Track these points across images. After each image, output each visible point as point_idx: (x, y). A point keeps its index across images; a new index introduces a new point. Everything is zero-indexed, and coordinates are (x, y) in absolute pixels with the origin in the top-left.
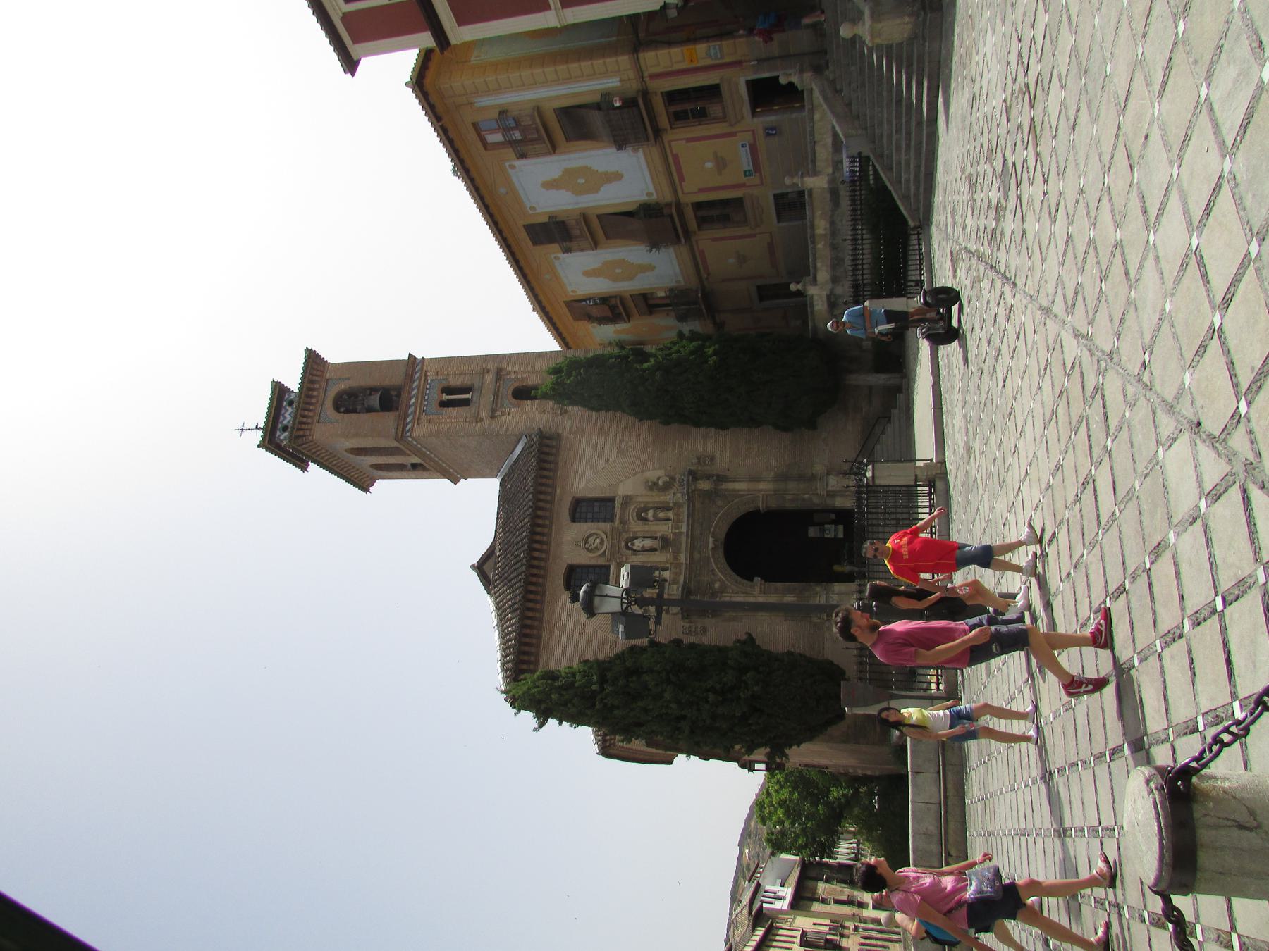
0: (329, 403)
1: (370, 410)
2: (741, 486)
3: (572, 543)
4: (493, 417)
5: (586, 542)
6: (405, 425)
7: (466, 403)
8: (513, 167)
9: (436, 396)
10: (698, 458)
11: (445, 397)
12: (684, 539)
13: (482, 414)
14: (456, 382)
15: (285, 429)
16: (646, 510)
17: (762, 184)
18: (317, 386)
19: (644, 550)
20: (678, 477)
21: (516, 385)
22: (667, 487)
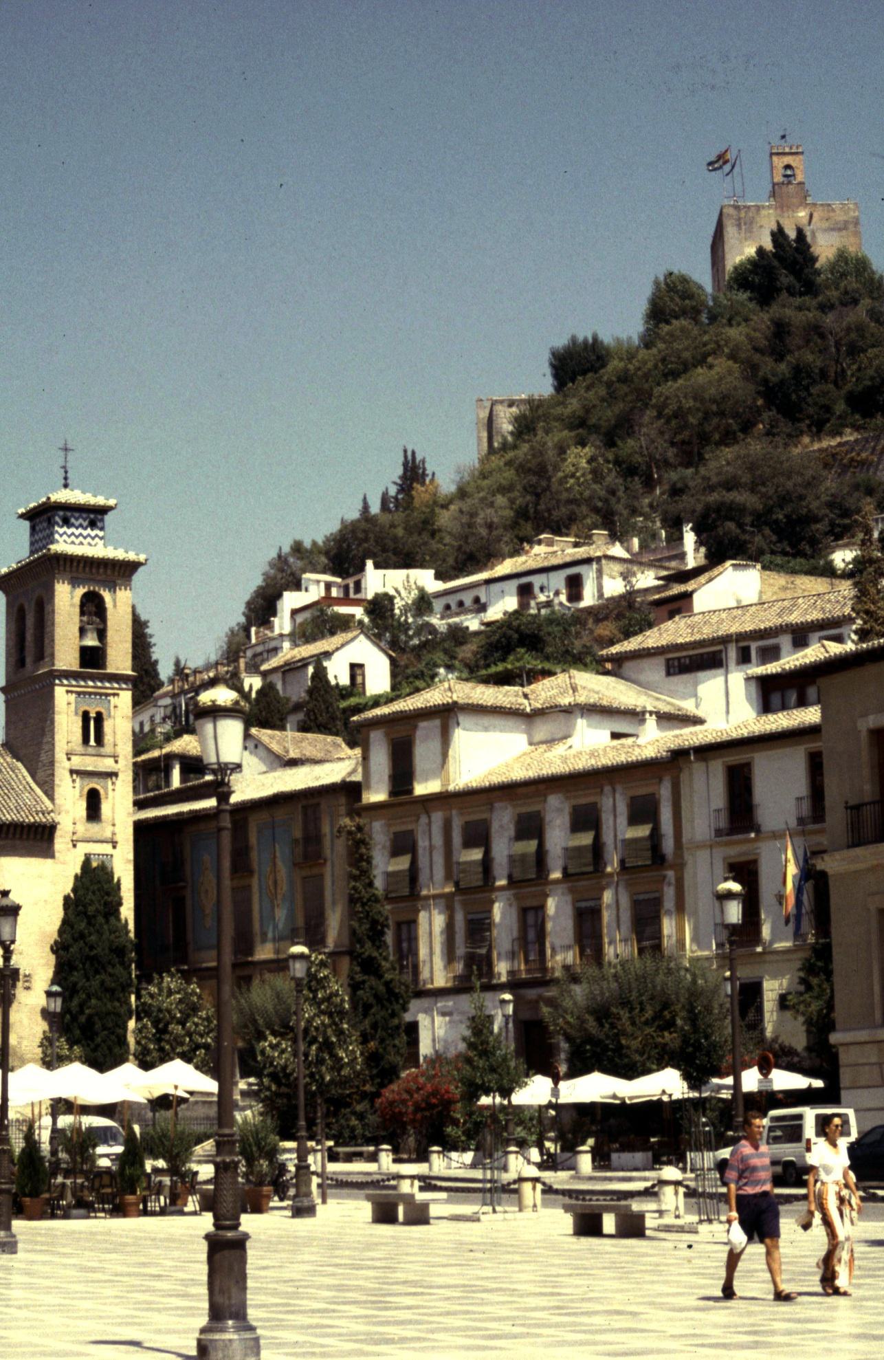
4: (72, 772)
7: (86, 740)
11: (93, 715)
13: (73, 758)
14: (108, 726)
18: (109, 572)
21: (102, 792)
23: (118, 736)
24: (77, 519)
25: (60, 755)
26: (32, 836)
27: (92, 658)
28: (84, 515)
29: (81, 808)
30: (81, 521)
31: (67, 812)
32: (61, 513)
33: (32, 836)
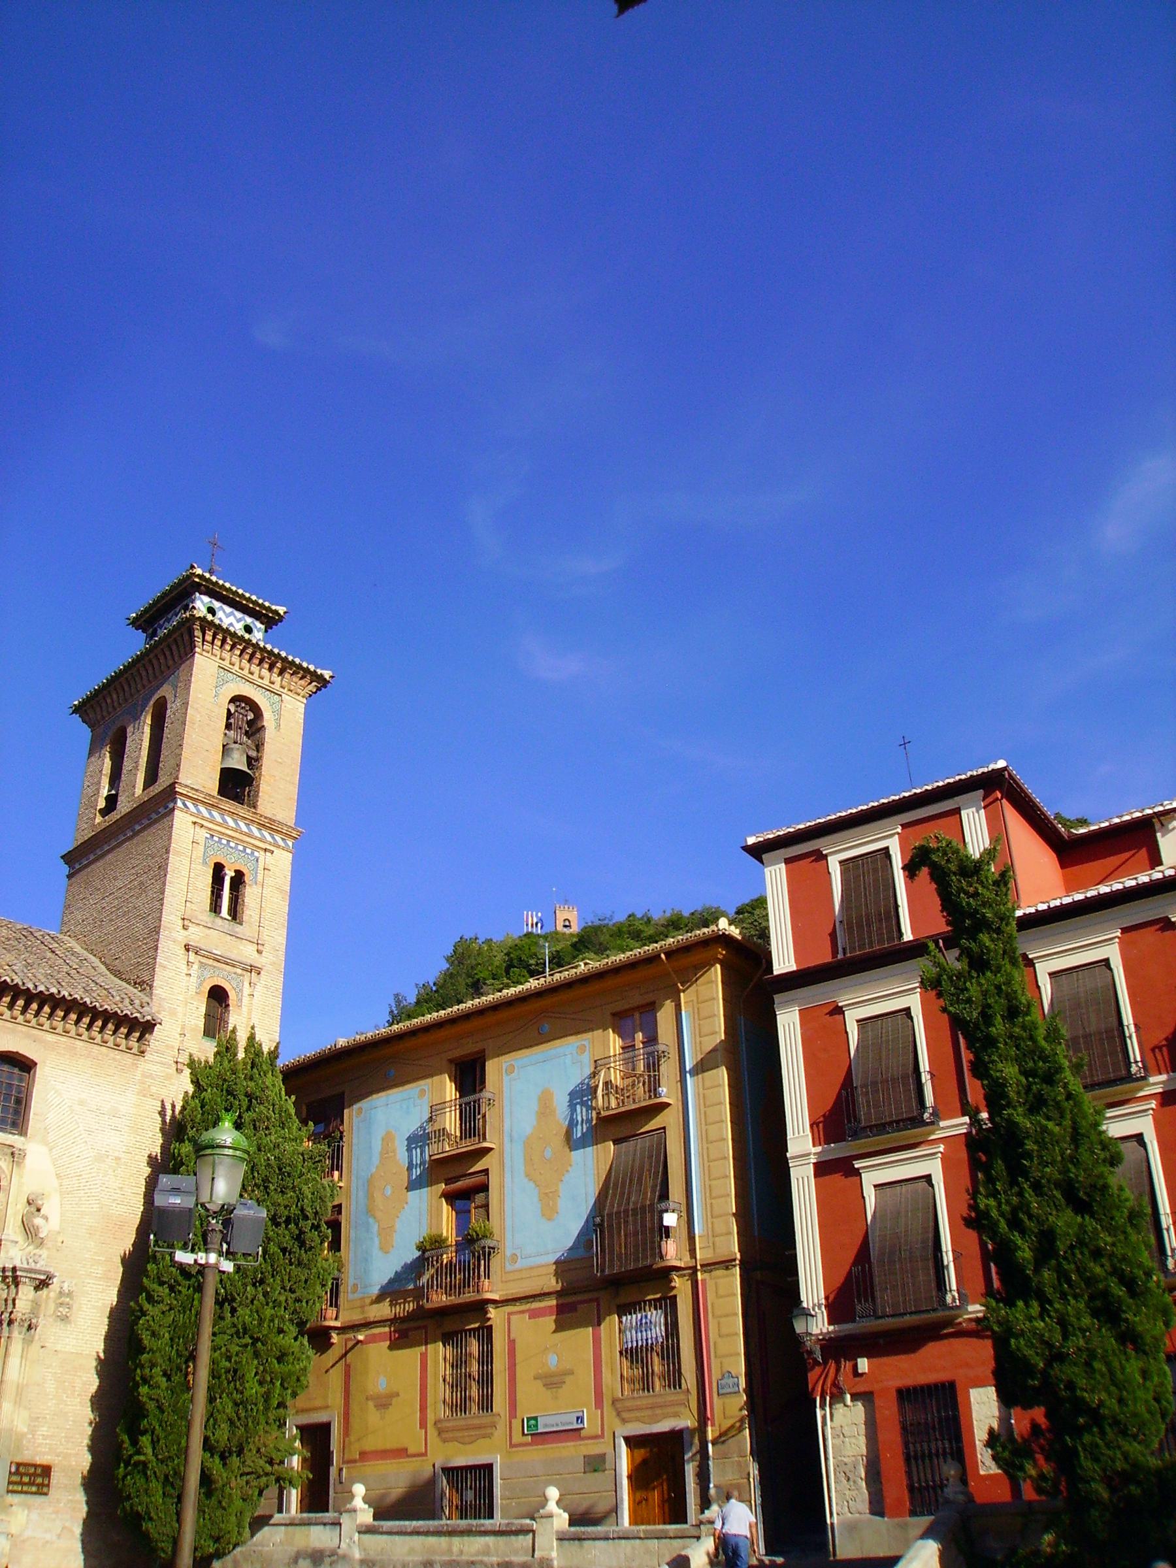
7: (215, 908)
8: (582, 1049)
10: (70, 1294)
11: (229, 874)
13: (193, 929)
14: (250, 894)
17: (512, 1446)
20: (44, 1252)
22: (30, 1231)
23: (266, 915)
24: (228, 616)
25: (171, 917)
27: (237, 785)
28: (239, 615)
32: (206, 599)
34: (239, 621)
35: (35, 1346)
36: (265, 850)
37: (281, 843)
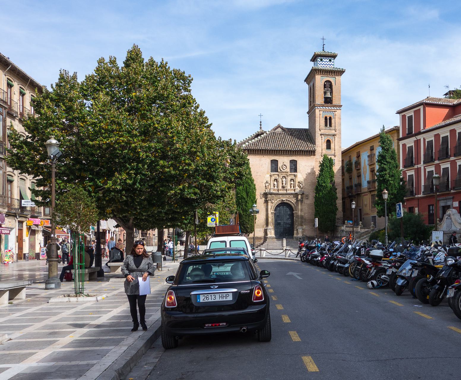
0: (328, 79)
1: (325, 93)
2: (300, 207)
3: (284, 161)
4: (321, 135)
5: (284, 165)
6: (319, 106)
7: (326, 125)
9: (328, 115)
10: (308, 195)
11: (328, 118)
12: (285, 192)
15: (321, 60)
16: (294, 181)
19: (282, 181)
21: (331, 141)
26: (308, 154)
28: (327, 58)
29: (325, 146)
30: (326, 60)
31: (320, 147)
32: (320, 58)
33: (308, 154)
34: (328, 60)
35: (303, 203)
36: (335, 111)
37: (338, 109)
